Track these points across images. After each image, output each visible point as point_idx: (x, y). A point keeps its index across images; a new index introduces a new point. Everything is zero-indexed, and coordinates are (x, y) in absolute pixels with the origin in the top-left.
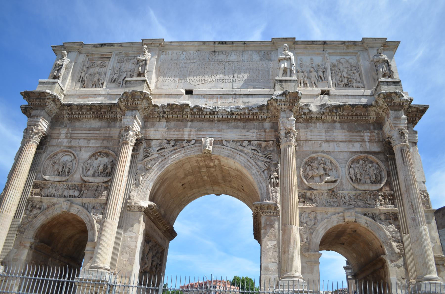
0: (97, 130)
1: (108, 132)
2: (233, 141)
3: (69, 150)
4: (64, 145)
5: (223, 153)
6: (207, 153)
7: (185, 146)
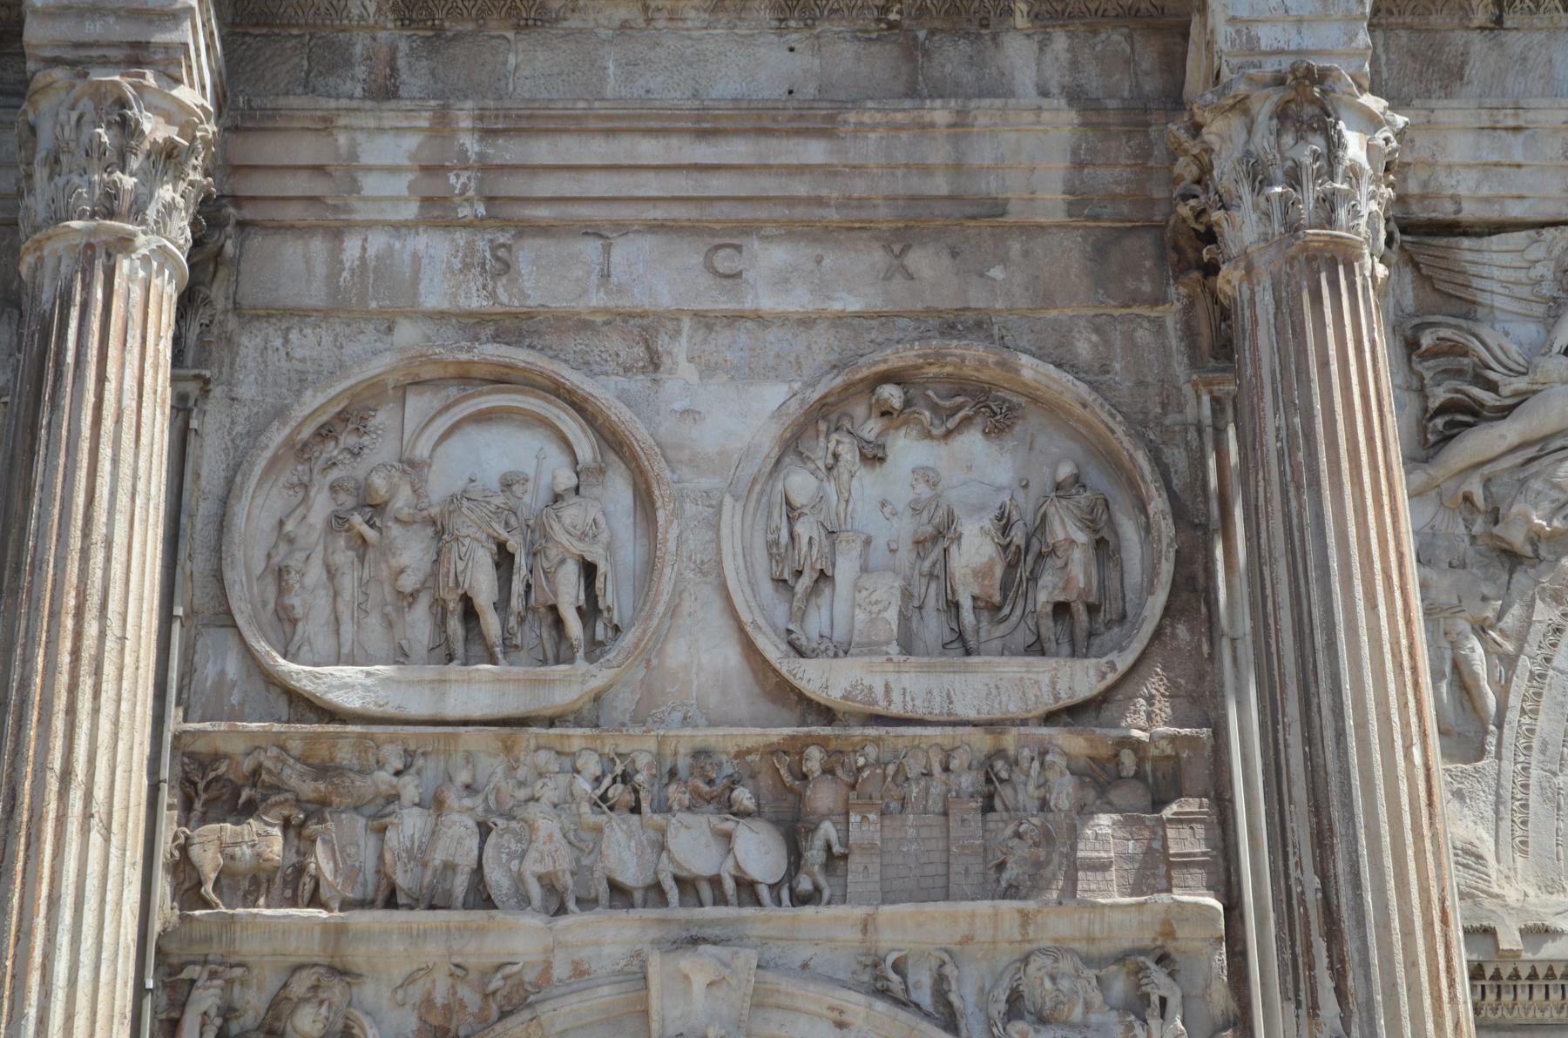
0: (799, 132)
1: (938, 152)
3: (520, 356)
4: (432, 299)
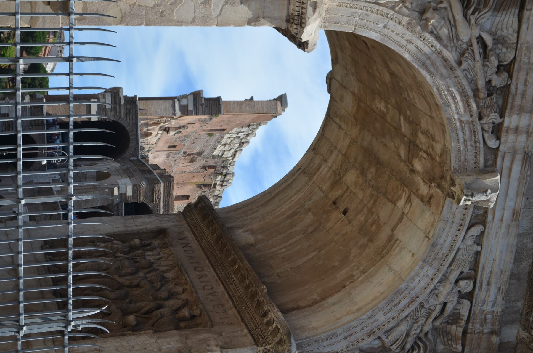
2: (478, 254)
5: (447, 230)
6: (452, 188)
7: (484, 121)
